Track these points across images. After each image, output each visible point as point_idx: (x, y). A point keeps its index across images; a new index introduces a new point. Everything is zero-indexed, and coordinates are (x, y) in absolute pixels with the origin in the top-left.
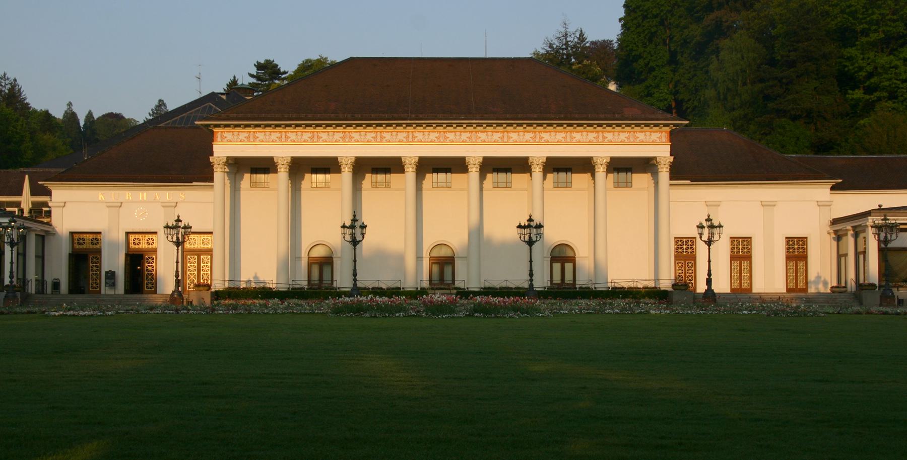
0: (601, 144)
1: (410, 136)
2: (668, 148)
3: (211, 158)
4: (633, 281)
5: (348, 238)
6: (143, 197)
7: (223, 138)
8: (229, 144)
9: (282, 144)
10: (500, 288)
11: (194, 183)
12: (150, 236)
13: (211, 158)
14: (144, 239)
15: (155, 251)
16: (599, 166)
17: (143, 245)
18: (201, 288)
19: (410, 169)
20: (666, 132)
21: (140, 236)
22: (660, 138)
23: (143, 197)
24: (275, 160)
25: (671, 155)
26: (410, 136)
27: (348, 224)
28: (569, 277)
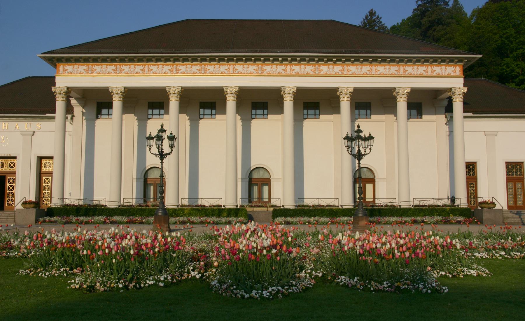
0: (403, 78)
1: (231, 69)
2: (462, 80)
3: (53, 88)
4: (433, 199)
5: (155, 150)
6: (5, 127)
7: (65, 70)
8: (70, 77)
9: (116, 78)
10: (313, 206)
11: (48, 115)
12: (12, 161)
13: (53, 88)
14: (7, 162)
15: (14, 173)
16: (401, 96)
17: (6, 168)
18: (28, 206)
19: (231, 98)
20: (459, 66)
21: (4, 161)
22: (455, 71)
23: (5, 127)
24: (110, 90)
25: (464, 86)
26: (231, 69)
27: (154, 133)
28: (369, 197)
